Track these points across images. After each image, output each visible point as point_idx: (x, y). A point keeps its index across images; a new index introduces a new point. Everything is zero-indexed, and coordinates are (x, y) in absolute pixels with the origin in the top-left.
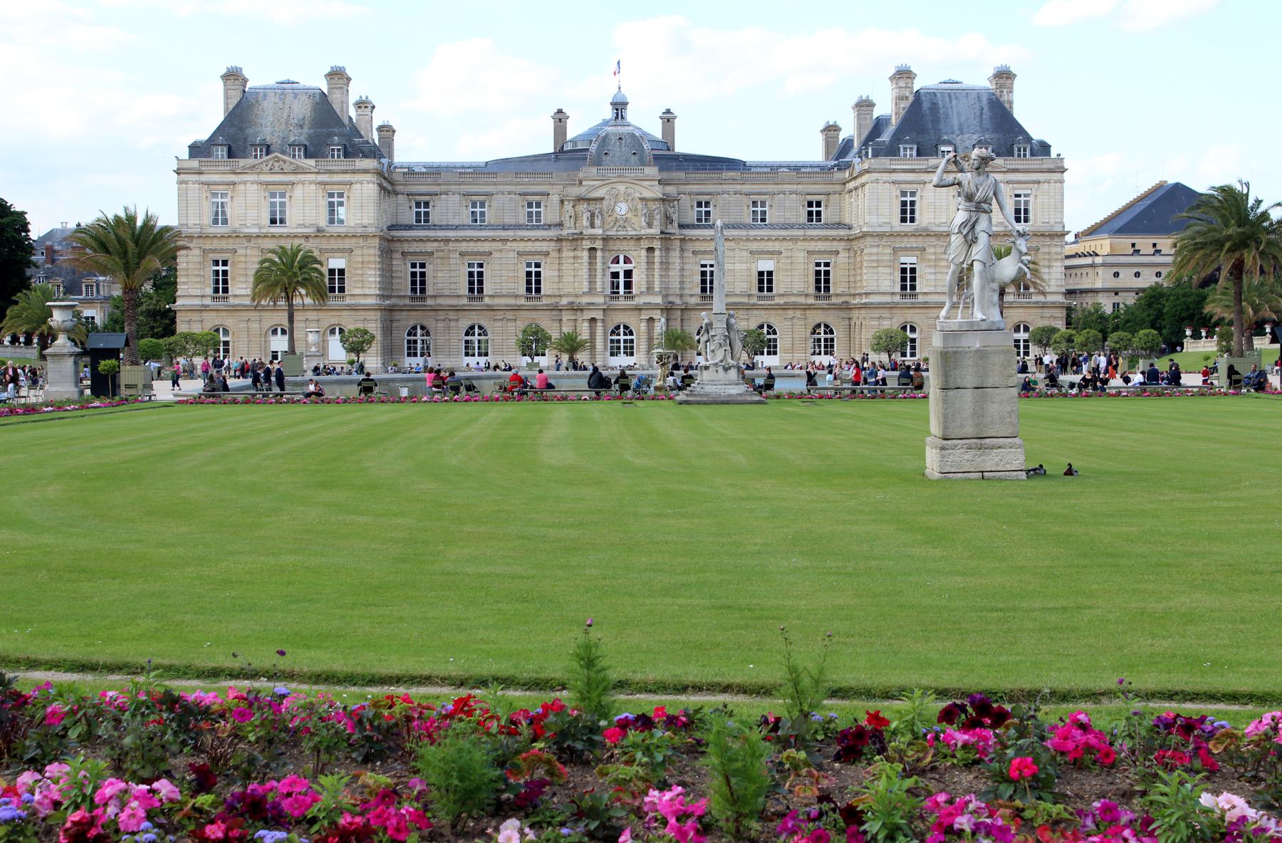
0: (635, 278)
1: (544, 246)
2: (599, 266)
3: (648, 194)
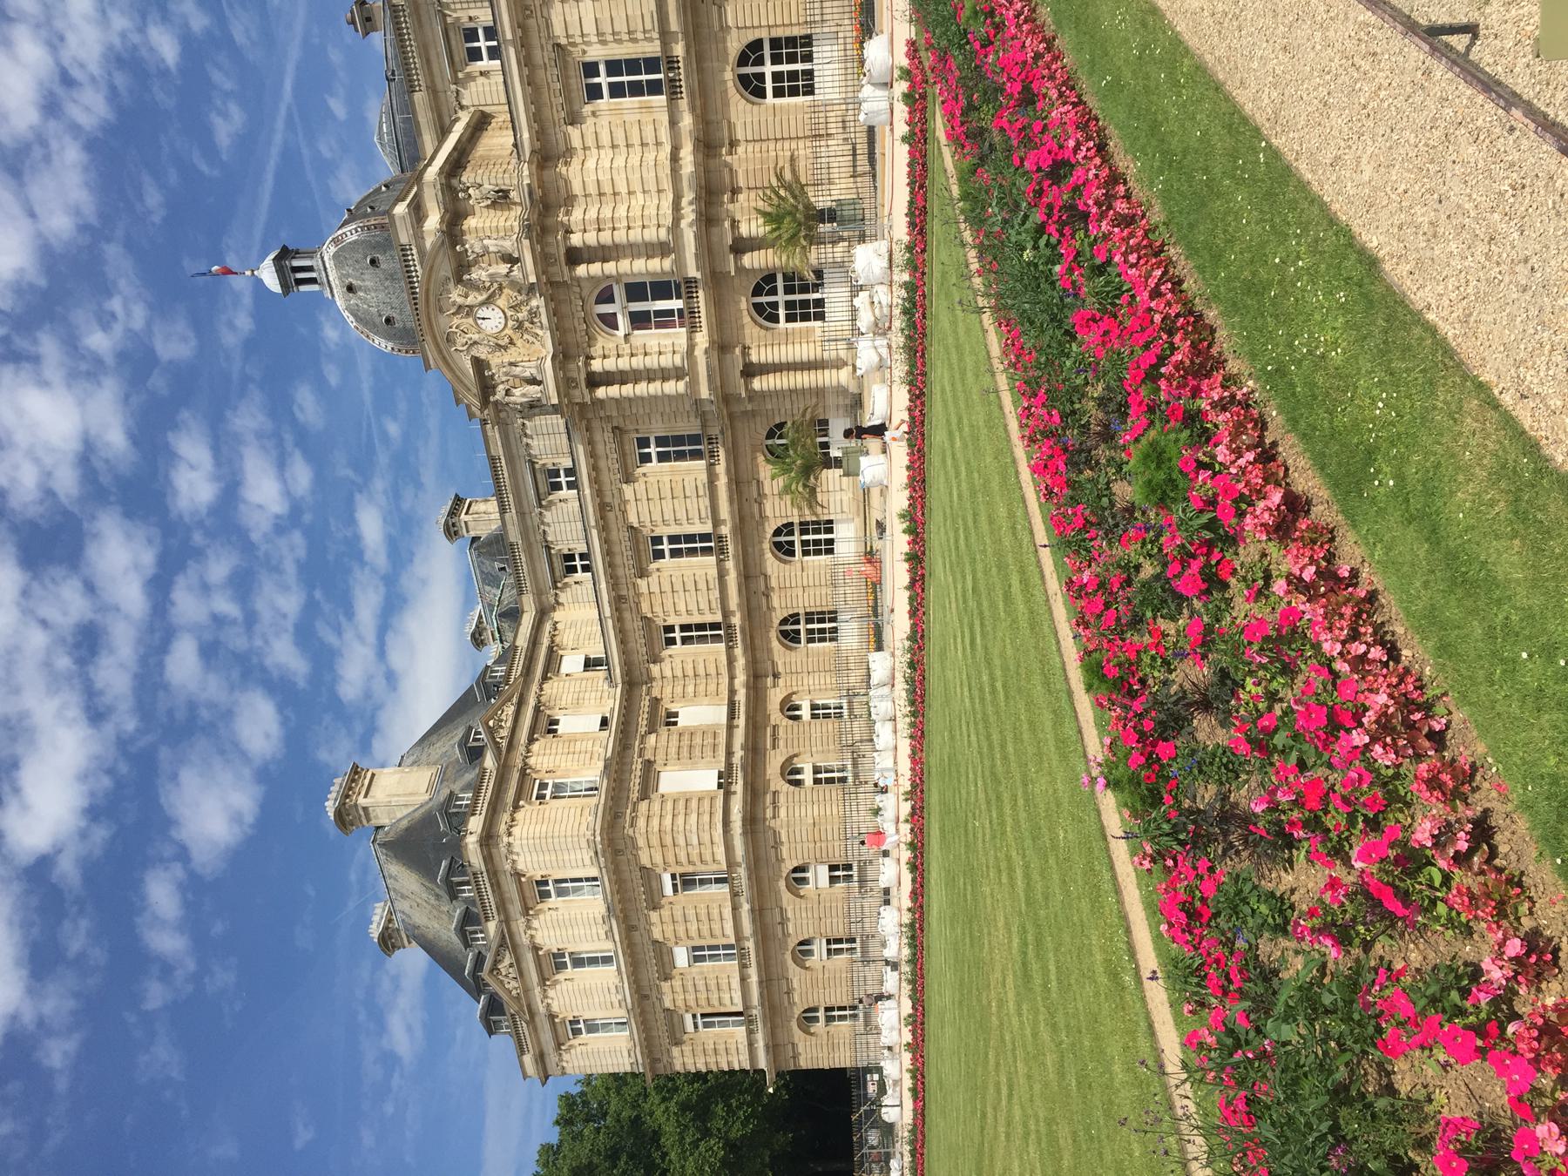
1: (604, 439)
2: (623, 363)
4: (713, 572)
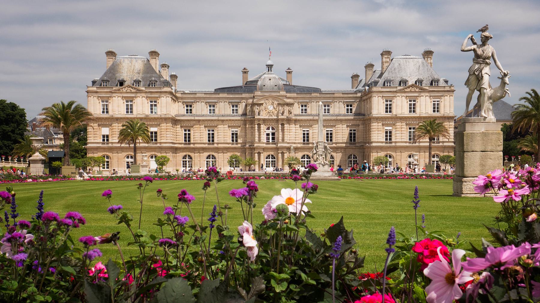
0: (276, 136)
3: (281, 102)
4: (205, 142)
